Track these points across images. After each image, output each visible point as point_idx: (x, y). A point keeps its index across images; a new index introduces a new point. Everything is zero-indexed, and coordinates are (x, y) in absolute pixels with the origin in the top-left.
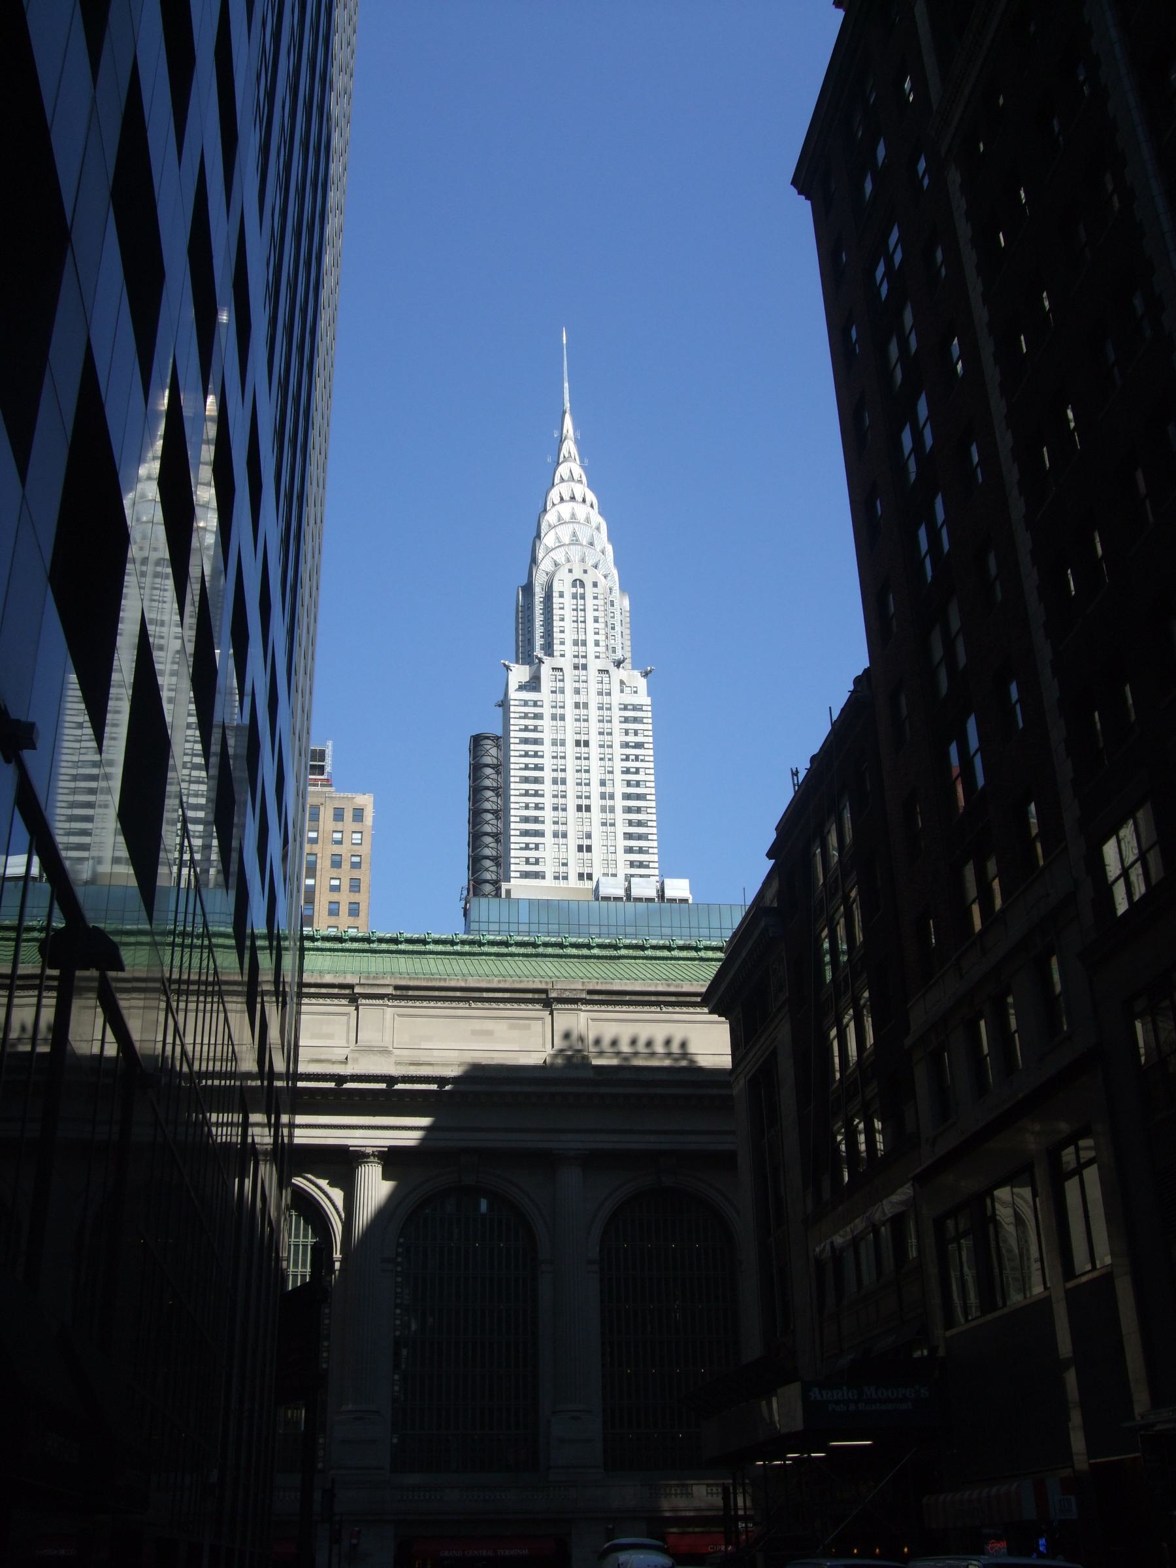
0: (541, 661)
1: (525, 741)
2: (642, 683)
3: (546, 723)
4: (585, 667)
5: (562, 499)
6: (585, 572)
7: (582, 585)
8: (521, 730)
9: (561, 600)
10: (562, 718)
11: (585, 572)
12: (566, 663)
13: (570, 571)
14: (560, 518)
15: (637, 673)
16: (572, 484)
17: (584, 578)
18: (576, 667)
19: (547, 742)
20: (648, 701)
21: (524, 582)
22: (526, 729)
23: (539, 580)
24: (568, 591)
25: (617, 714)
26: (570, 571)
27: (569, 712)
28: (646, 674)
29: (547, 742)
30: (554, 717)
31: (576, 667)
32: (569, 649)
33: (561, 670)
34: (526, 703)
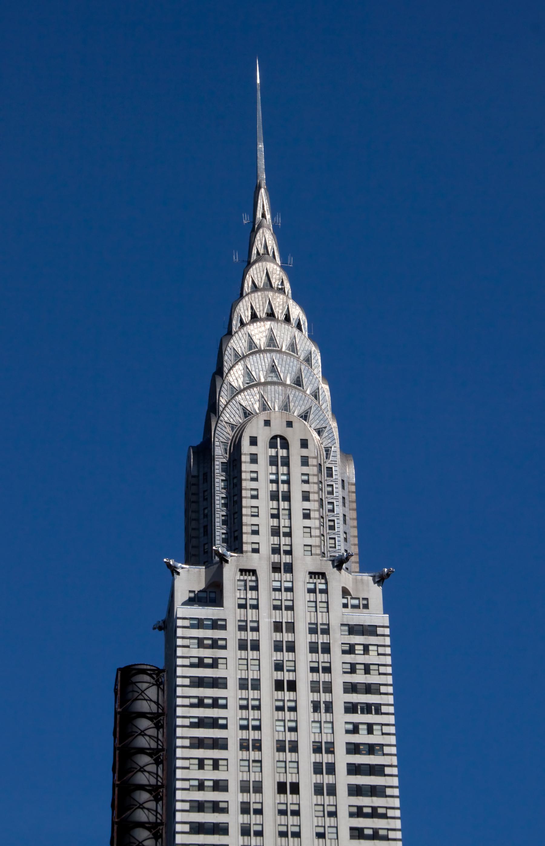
0: (223, 560)
1: (199, 682)
2: (375, 594)
3: (232, 653)
4: (289, 568)
5: (254, 317)
6: (290, 424)
7: (285, 445)
8: (192, 665)
9: (254, 467)
10: (256, 646)
11: (290, 424)
12: (261, 562)
13: (267, 423)
14: (251, 343)
15: (367, 578)
16: (270, 294)
17: (288, 433)
18: (276, 568)
19: (233, 684)
20: (385, 620)
21: (198, 440)
22: (201, 663)
23: (221, 437)
24: (263, 451)
25: (338, 638)
26: (267, 423)
27: (266, 637)
28: (380, 580)
29: (233, 684)
30: (242, 646)
31: (276, 568)
32: (265, 541)
33: (253, 572)
34: (199, 624)
